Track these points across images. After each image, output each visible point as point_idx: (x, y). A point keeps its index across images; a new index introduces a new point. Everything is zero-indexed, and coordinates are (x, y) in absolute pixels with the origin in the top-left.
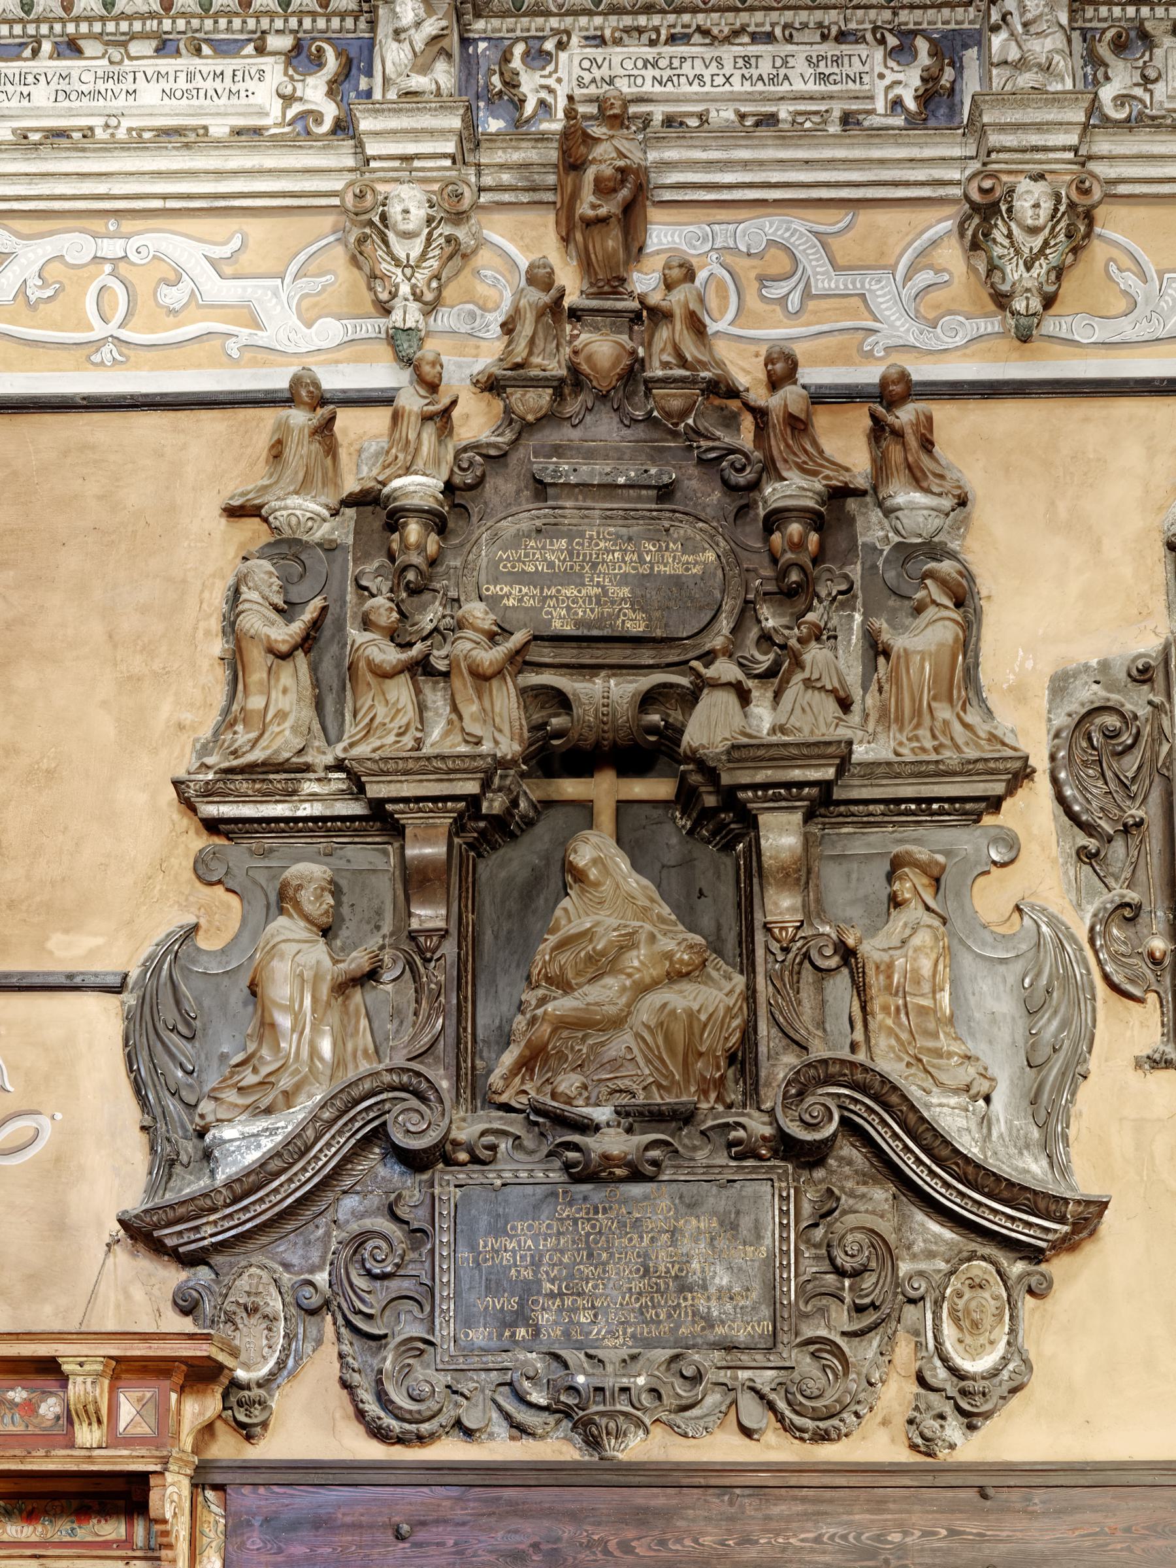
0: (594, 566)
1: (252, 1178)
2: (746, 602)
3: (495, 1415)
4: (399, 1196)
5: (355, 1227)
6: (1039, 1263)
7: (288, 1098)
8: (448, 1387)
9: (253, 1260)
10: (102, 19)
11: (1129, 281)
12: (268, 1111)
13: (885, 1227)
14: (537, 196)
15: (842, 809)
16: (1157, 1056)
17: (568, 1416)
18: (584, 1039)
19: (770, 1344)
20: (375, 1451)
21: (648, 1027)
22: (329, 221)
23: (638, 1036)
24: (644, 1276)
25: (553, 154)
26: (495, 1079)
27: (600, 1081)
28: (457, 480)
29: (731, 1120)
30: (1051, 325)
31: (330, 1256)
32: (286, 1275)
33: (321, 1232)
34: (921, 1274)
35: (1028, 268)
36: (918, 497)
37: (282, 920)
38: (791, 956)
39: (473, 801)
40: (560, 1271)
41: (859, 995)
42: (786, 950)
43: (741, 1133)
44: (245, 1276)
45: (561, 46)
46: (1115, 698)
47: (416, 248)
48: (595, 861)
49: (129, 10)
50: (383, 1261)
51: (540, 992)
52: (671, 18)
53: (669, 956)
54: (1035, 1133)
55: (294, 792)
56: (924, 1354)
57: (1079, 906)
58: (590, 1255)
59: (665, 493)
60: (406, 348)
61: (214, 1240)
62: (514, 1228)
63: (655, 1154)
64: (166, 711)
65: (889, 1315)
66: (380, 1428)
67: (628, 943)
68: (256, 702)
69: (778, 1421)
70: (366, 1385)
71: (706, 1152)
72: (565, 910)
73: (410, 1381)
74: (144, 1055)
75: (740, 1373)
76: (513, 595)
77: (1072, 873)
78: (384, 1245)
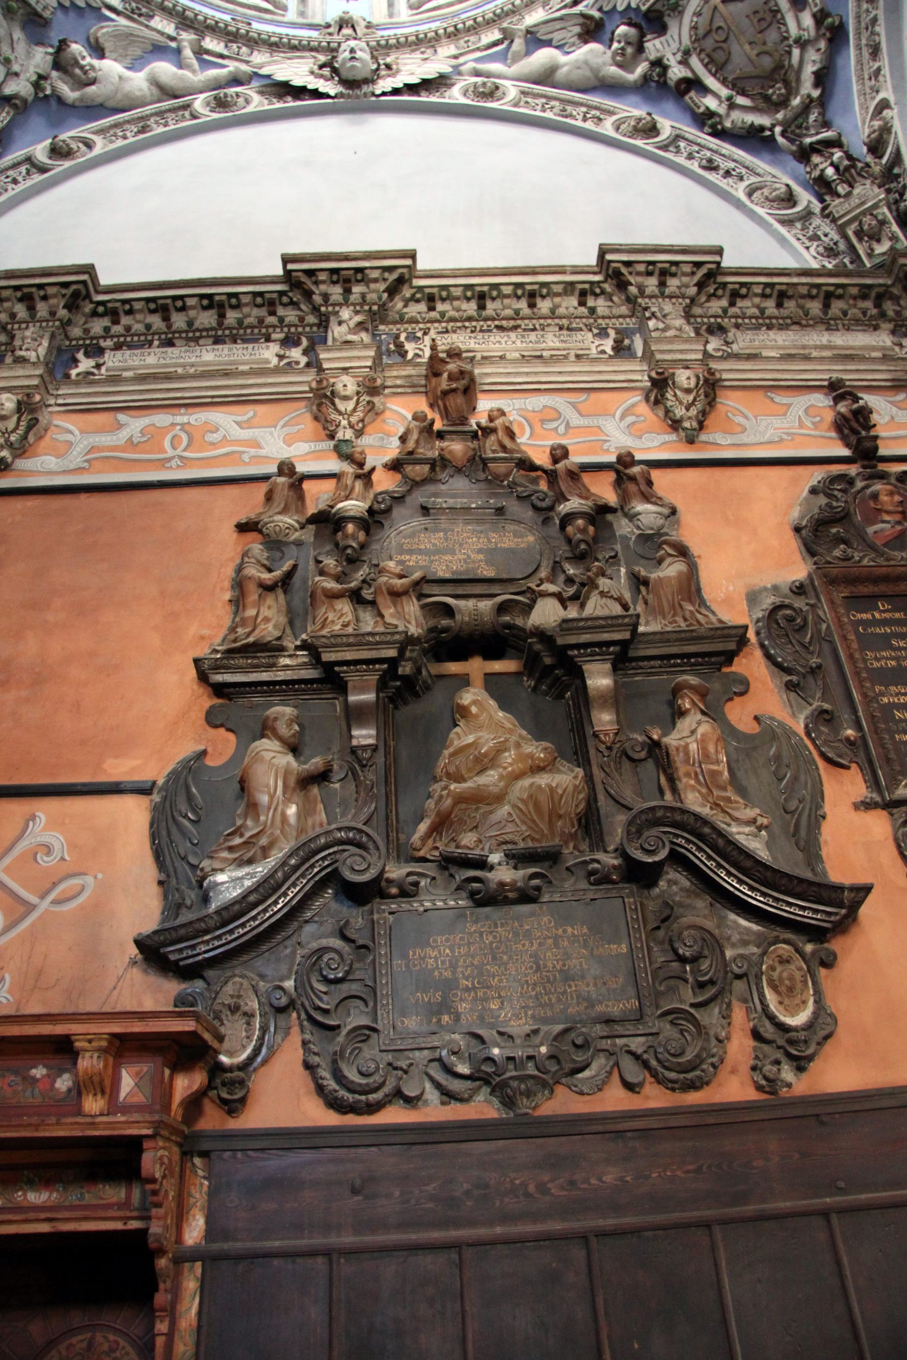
0: (461, 545)
1: (237, 907)
2: (555, 562)
3: (428, 1085)
4: (347, 922)
5: (315, 945)
6: (822, 943)
7: (265, 852)
8: (390, 1064)
9: (237, 972)
10: (187, 332)
11: (741, 420)
12: (250, 862)
13: (709, 924)
14: (415, 389)
15: (634, 664)
16: (868, 800)
17: (487, 1082)
18: (477, 809)
19: (638, 1017)
20: (332, 1119)
21: (522, 800)
22: (303, 404)
23: (514, 806)
24: (536, 971)
25: (423, 371)
26: (416, 838)
27: (491, 837)
28: (376, 506)
29: (587, 858)
30: (703, 437)
31: (296, 968)
32: (262, 983)
33: (288, 951)
34: (742, 956)
35: (687, 409)
36: (650, 507)
37: (264, 740)
38: (615, 751)
39: (393, 663)
40: (472, 971)
41: (665, 772)
42: (609, 748)
43: (596, 865)
44: (230, 984)
45: (425, 334)
46: (787, 601)
47: (350, 405)
48: (475, 702)
49: (201, 327)
50: (336, 969)
51: (443, 784)
52: (482, 323)
53: (531, 756)
54: (800, 854)
55: (273, 665)
56: (755, 1015)
57: (794, 715)
58: (494, 958)
59: (500, 511)
60: (345, 449)
61: (206, 956)
62: (435, 941)
63: (536, 882)
64: (194, 629)
65: (723, 988)
66: (336, 1098)
67: (500, 749)
68: (251, 612)
69: (652, 1076)
70: (324, 1066)
71: (572, 881)
72: (457, 733)
73: (360, 1061)
74: (164, 833)
75: (617, 1040)
76: (412, 560)
77: (785, 697)
78: (336, 957)
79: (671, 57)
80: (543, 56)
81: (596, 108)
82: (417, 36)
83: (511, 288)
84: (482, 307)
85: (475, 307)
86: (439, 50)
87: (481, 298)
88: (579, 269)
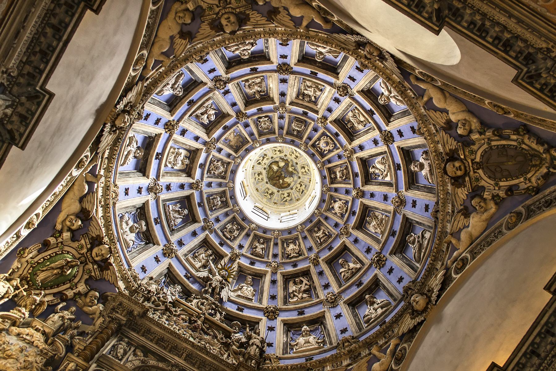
52: (546, 362)
79: (495, 191)
80: (463, 235)
81: (496, 229)
82: (427, 271)
83: (538, 338)
84: (538, 356)
85: (537, 358)
86: (437, 267)
87: (534, 353)
88: (550, 304)
